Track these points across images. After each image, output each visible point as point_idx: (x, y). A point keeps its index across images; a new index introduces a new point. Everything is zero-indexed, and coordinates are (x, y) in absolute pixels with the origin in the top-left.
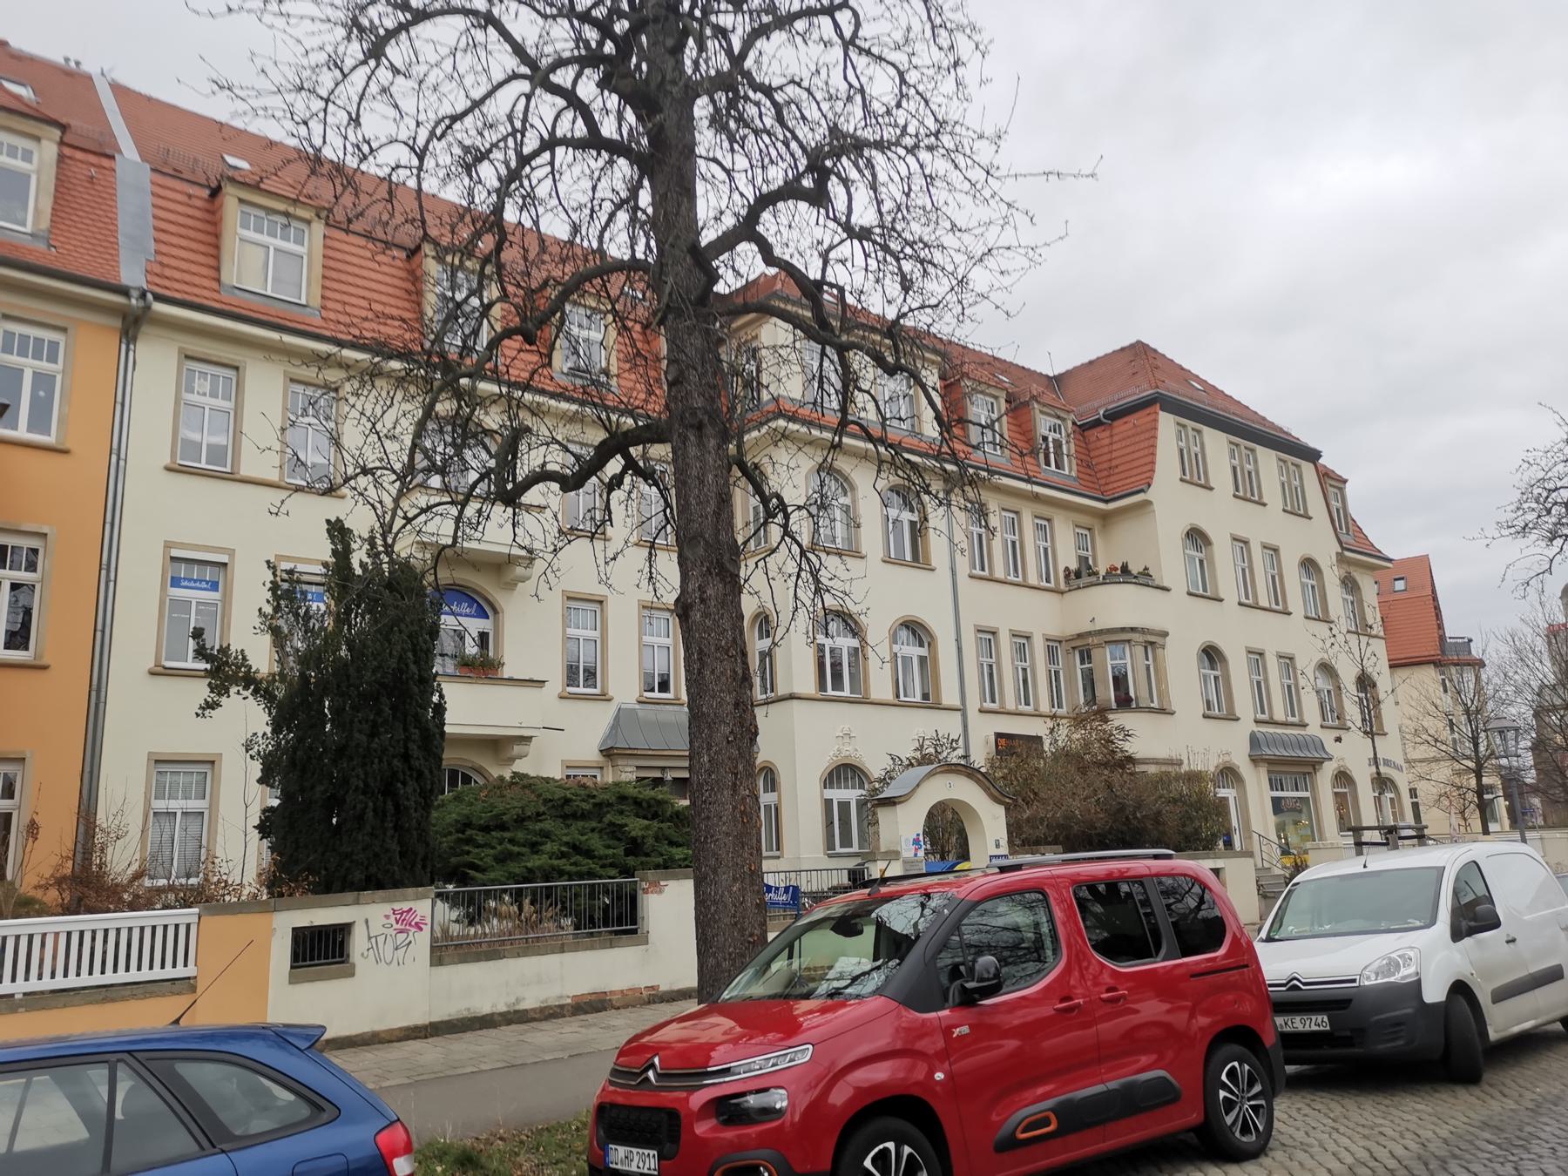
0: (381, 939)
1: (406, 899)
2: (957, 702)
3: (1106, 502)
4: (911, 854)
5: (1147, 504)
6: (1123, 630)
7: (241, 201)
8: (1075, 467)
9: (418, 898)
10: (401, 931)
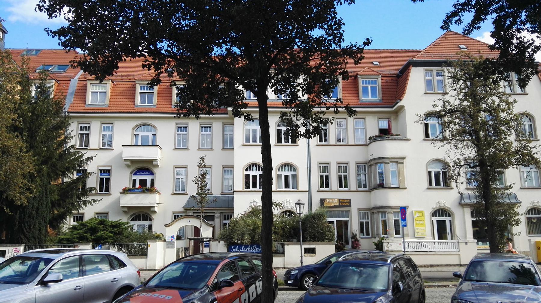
0: (11, 254)
1: (16, 246)
2: (306, 188)
3: (392, 107)
4: (170, 241)
5: (403, 107)
6: (379, 158)
7: (91, 83)
8: (381, 96)
9: (18, 246)
10: (15, 252)
